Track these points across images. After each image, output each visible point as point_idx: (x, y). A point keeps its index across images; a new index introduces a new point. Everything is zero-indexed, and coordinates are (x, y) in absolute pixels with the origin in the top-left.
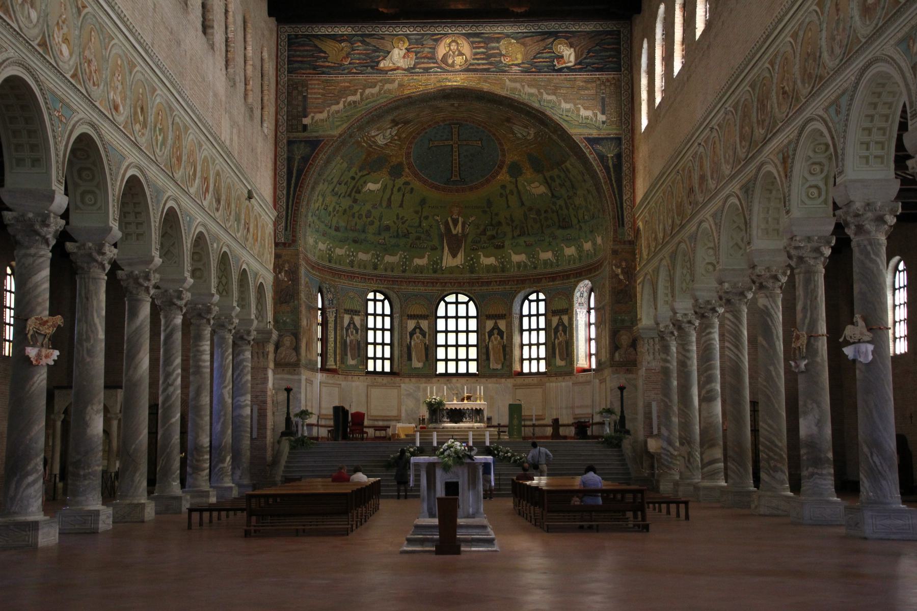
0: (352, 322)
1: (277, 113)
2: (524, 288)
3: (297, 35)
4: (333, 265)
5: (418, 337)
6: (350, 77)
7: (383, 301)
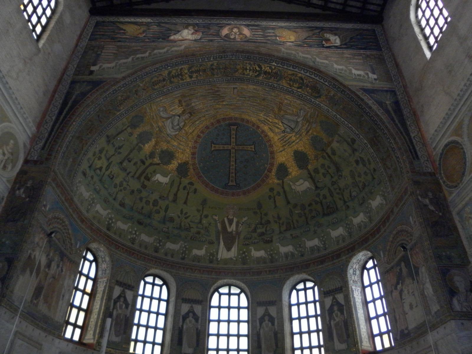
0: (122, 296)
1: (68, 63)
2: (292, 275)
3: (104, 22)
5: (190, 322)
6: (142, 44)
7: (161, 286)
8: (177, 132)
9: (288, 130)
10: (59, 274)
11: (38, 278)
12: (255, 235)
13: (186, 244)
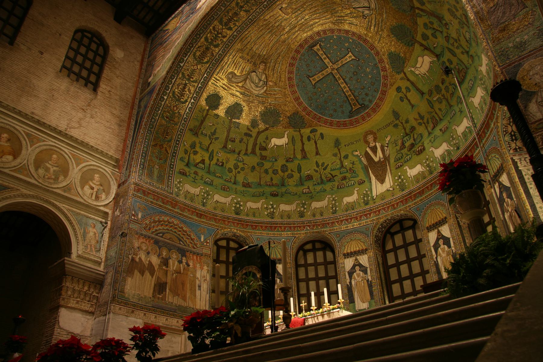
3: (155, 35)
4: (241, 217)
5: (358, 275)
8: (265, 88)
9: (367, 12)
10: (184, 269)
11: (154, 277)
12: (405, 151)
13: (334, 196)
